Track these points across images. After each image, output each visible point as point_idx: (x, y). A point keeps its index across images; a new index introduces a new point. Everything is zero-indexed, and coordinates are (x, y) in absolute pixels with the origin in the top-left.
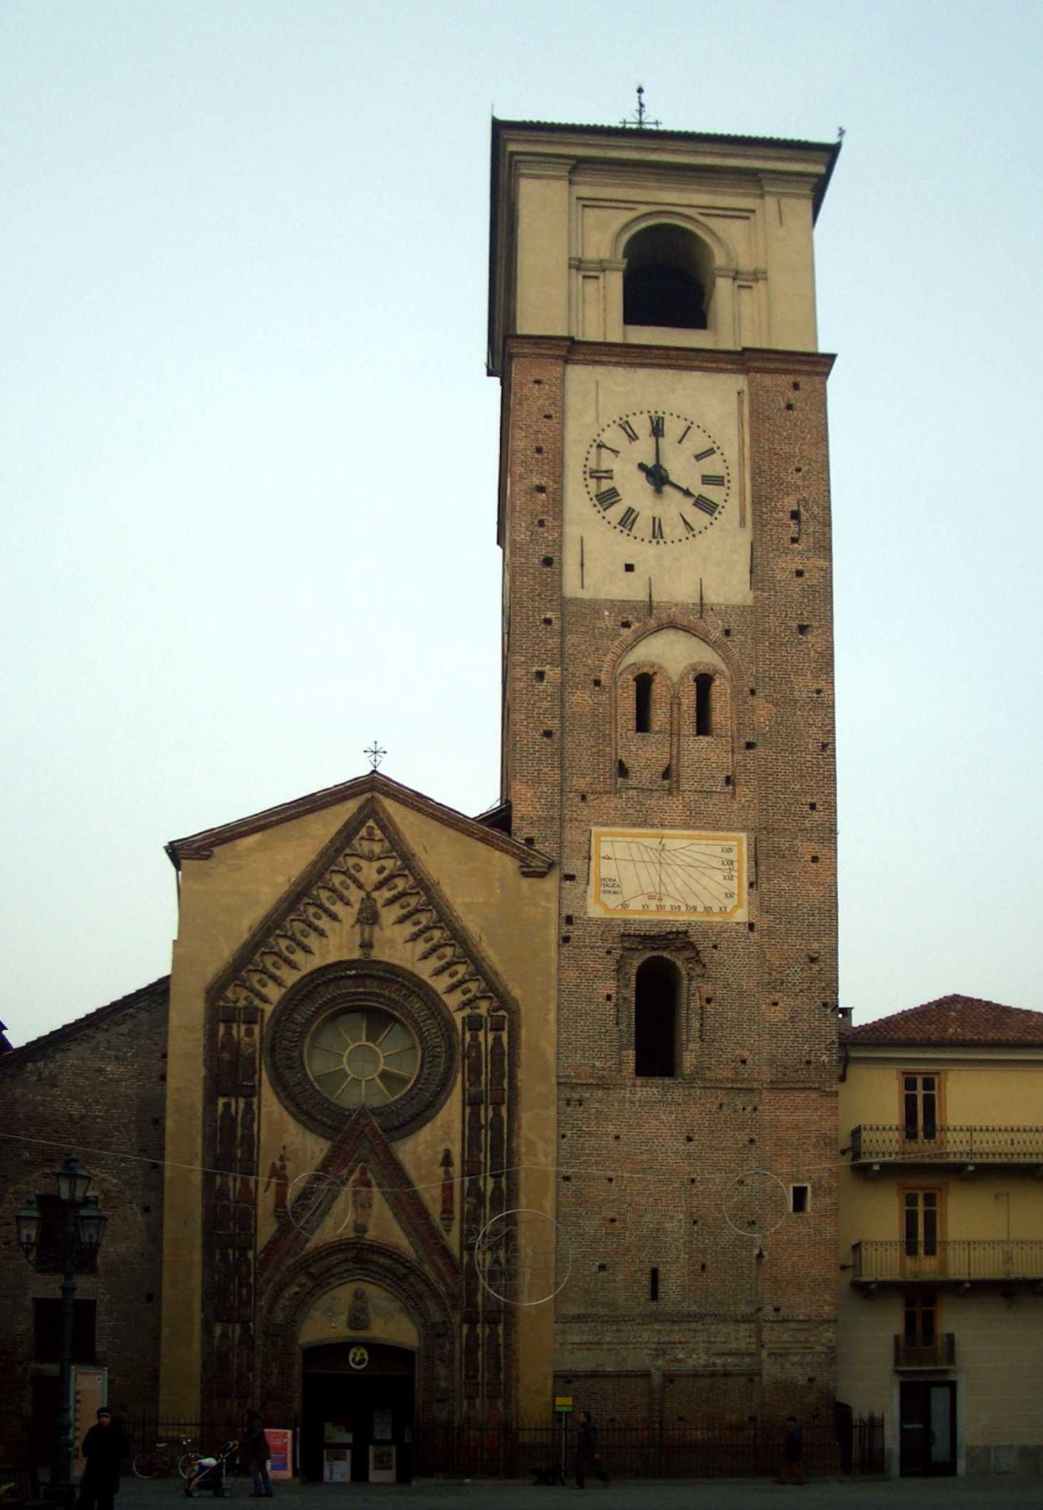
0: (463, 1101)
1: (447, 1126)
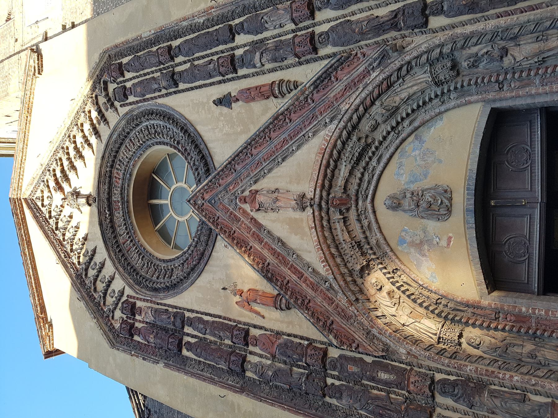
0: (175, 93)
1: (193, 105)
